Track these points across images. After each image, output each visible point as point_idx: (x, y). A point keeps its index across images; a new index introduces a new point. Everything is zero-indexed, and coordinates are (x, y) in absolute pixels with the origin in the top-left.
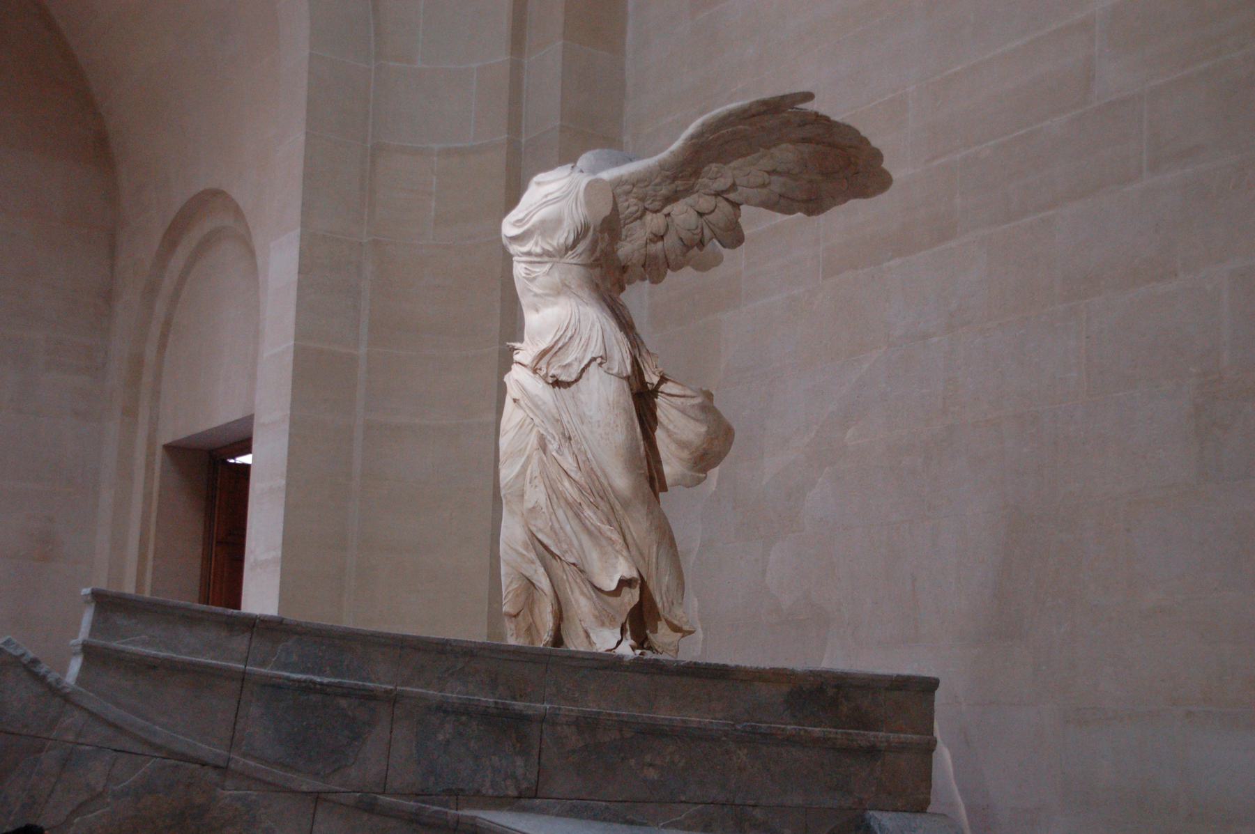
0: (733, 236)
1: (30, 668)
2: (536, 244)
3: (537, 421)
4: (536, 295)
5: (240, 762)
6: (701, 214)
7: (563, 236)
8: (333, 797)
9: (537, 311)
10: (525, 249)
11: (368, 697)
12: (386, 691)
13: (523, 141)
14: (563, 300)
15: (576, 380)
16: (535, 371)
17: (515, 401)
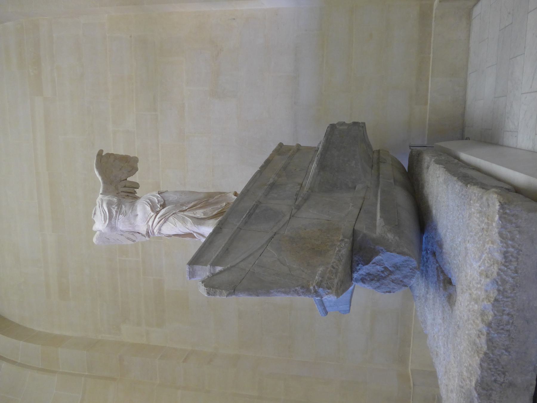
0: (136, 186)
1: (214, 275)
2: (114, 208)
3: (174, 212)
4: (131, 213)
5: (275, 230)
6: (125, 187)
7: (115, 200)
8: (293, 213)
9: (137, 215)
10: (114, 213)
11: (256, 206)
12: (256, 202)
13: (87, 374)
14: (136, 204)
15: (165, 201)
16: (157, 213)
17: (165, 222)
